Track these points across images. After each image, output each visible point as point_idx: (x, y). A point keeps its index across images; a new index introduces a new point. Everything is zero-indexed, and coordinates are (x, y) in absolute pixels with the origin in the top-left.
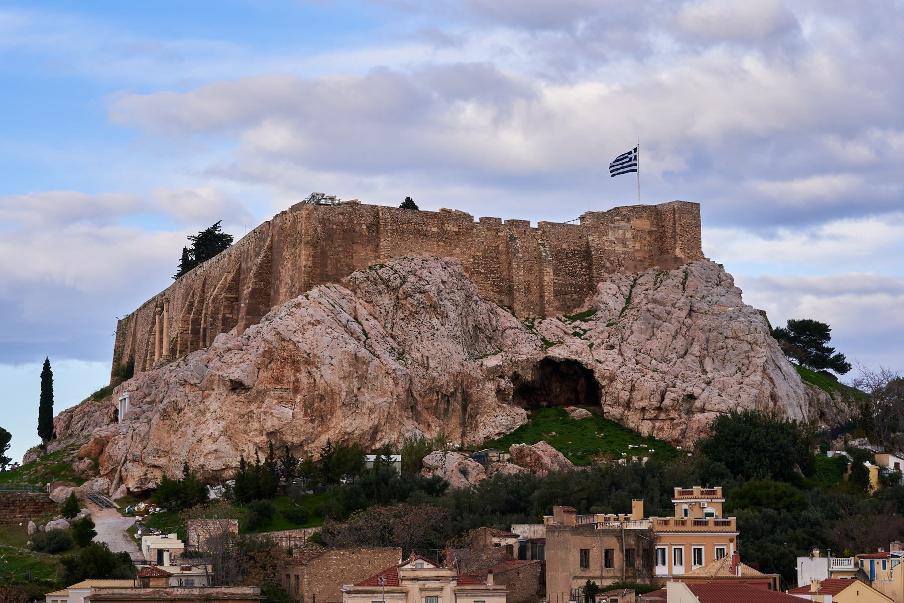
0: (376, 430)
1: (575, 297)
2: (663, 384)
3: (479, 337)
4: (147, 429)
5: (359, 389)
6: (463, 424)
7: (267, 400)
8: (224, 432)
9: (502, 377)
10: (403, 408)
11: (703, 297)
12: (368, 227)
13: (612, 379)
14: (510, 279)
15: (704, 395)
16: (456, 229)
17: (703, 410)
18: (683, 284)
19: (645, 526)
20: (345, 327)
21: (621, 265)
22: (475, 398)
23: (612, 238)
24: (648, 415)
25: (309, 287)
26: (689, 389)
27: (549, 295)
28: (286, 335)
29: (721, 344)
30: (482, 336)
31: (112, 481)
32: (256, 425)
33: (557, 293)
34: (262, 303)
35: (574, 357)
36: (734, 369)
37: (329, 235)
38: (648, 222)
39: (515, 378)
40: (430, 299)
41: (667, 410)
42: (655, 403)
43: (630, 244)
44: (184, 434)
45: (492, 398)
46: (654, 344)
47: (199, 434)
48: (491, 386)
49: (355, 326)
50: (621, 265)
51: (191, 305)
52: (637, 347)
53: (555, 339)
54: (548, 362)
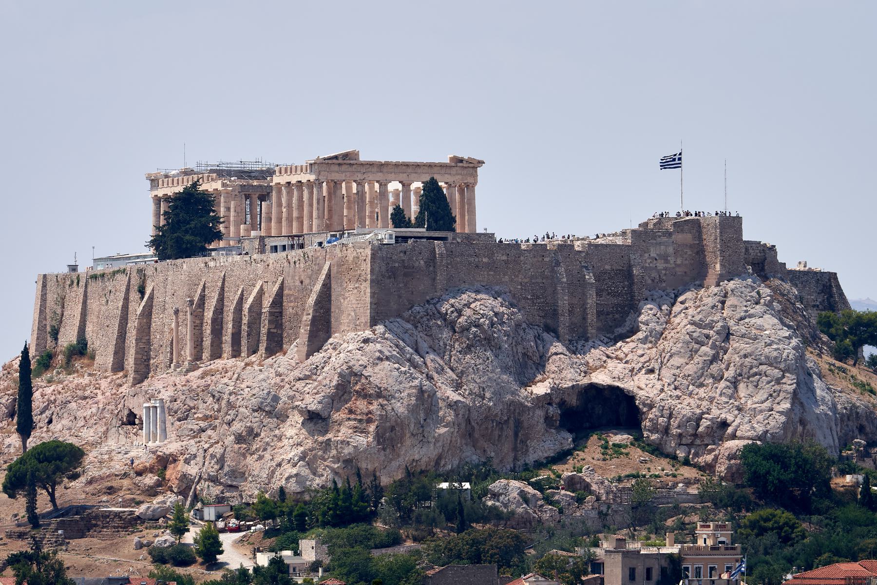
0: (440, 458)
1: (617, 316)
2: (698, 411)
4: (222, 451)
5: (425, 420)
6: (515, 449)
7: (343, 430)
8: (302, 458)
9: (550, 404)
10: (463, 436)
11: (741, 319)
12: (425, 262)
13: (651, 406)
14: (555, 304)
16: (504, 258)
17: (734, 437)
18: (723, 303)
19: (675, 550)
20: (409, 360)
21: (661, 281)
22: (525, 424)
23: (653, 255)
24: (684, 441)
25: (374, 322)
26: (723, 416)
27: (591, 317)
28: (356, 368)
29: (755, 370)
30: (530, 363)
31: (186, 498)
32: (334, 452)
33: (599, 314)
34: (321, 329)
35: (617, 384)
36: (765, 396)
37: (392, 273)
38: (689, 236)
39: (562, 404)
40: (484, 331)
41: (702, 437)
42: (691, 431)
43: (672, 259)
44: (261, 458)
45: (541, 426)
47: (278, 459)
48: (540, 413)
49: (417, 358)
50: (661, 281)
51: (202, 298)
52: (677, 372)
53: (598, 363)
54: (593, 386)
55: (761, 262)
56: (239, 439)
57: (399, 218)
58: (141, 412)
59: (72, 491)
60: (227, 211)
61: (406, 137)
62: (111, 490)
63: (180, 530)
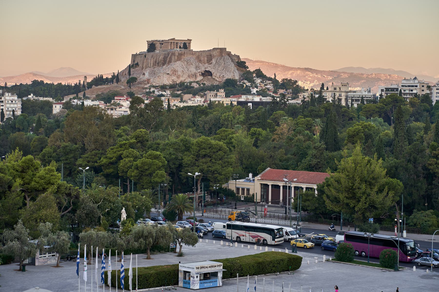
3: (197, 67)
34: (170, 62)
55: (229, 54)
60: (158, 45)
61: (181, 36)
63: (150, 89)
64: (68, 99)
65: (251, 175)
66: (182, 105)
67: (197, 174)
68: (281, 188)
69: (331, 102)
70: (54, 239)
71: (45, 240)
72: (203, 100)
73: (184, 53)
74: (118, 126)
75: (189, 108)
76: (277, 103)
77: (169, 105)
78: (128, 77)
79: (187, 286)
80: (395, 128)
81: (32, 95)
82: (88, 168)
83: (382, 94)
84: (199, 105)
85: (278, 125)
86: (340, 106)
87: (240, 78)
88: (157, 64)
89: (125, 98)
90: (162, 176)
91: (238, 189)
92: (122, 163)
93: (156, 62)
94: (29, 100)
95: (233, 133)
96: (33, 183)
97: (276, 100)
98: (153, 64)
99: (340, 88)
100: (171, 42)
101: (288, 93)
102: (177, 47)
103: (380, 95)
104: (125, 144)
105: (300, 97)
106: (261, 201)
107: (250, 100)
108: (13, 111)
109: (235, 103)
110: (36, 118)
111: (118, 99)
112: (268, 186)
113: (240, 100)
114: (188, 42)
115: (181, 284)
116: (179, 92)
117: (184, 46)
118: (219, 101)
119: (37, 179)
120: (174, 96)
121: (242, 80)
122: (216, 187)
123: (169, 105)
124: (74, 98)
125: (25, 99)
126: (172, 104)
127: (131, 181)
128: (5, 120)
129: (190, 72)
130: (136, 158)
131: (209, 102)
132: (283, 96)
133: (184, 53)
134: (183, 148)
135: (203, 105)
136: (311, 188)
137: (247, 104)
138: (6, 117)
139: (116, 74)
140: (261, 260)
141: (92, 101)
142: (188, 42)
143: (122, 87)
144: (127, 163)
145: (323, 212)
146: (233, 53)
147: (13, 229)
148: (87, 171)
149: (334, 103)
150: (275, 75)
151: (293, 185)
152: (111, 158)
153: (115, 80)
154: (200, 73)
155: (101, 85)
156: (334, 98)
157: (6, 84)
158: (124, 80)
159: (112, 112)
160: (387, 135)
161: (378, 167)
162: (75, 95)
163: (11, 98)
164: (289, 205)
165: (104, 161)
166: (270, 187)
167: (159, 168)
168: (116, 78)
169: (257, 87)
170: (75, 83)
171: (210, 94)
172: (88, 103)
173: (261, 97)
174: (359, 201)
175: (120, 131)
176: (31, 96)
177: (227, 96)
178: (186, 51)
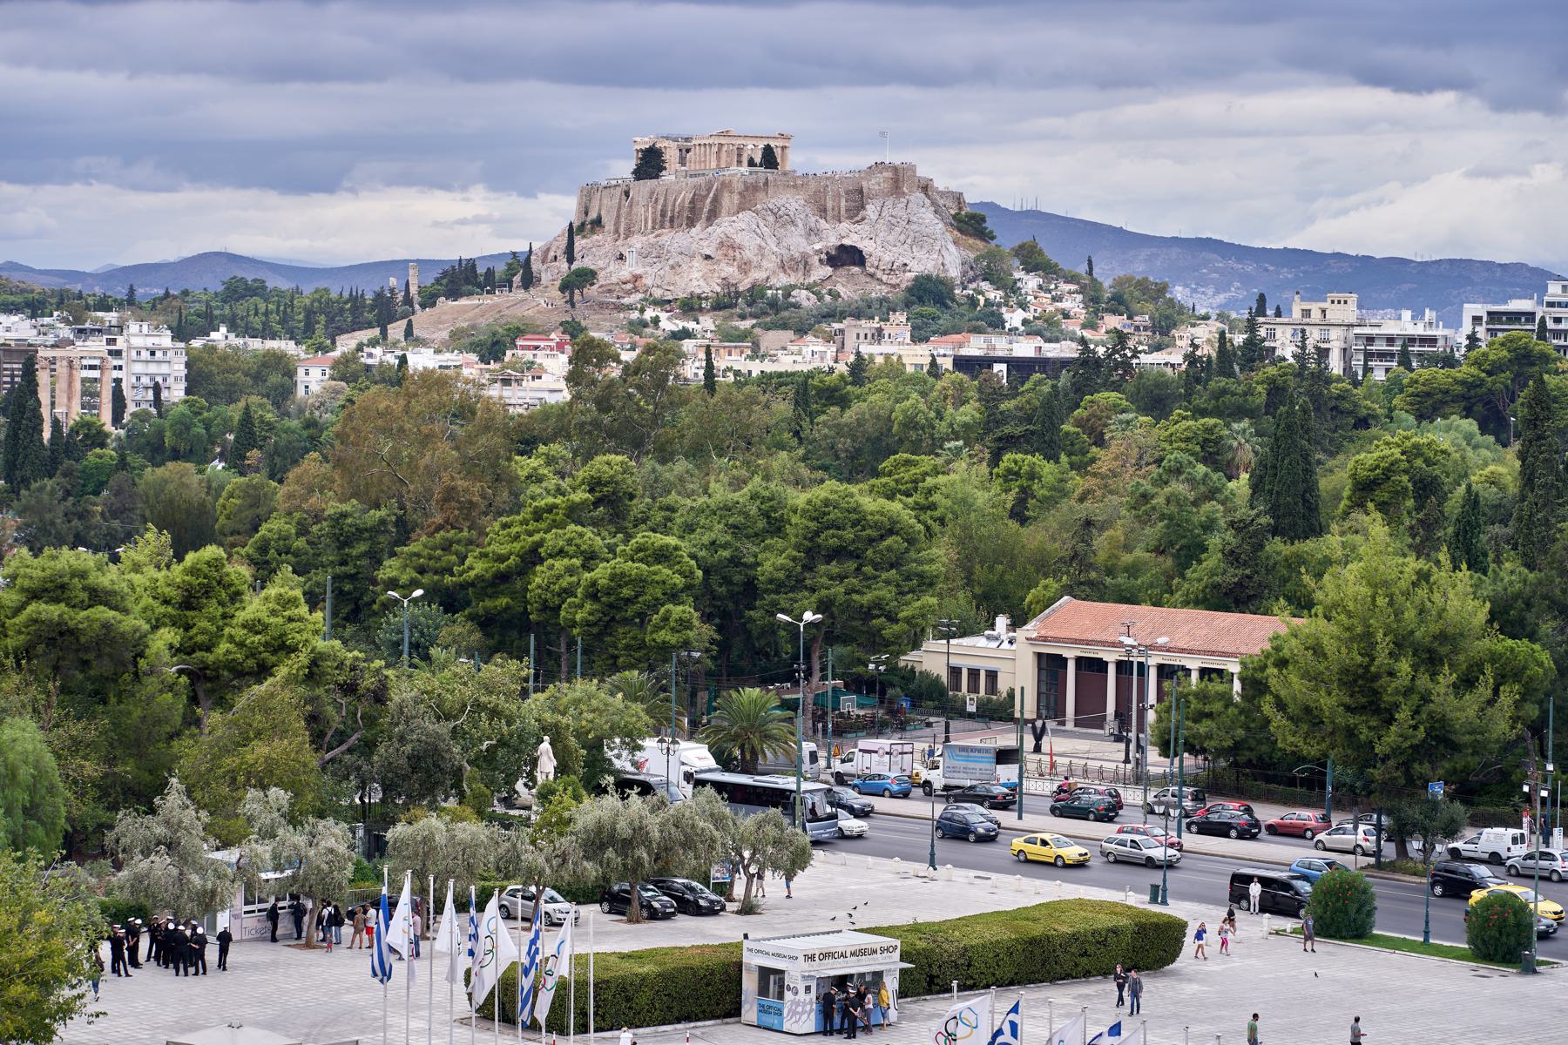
15: (913, 265)
34: (713, 215)
46: (890, 238)
55: (926, 188)
56: (672, 267)
57: (751, 163)
58: (626, 254)
59: (592, 291)
60: (671, 155)
62: (610, 291)
63: (642, 311)
64: (353, 344)
65: (1002, 622)
66: (756, 368)
67: (808, 616)
68: (1112, 670)
69: (1291, 360)
70: (295, 847)
71: (265, 850)
72: (831, 350)
73: (766, 183)
74: (527, 443)
75: (782, 379)
76: (1098, 363)
77: (709, 367)
78: (563, 265)
79: (770, 1020)
80: (1522, 456)
81: (223, 329)
82: (418, 593)
83: (1474, 333)
84: (820, 371)
85: (1100, 442)
86: (1322, 377)
87: (964, 274)
88: (667, 219)
89: (552, 344)
90: (684, 624)
91: (955, 672)
92: (540, 577)
93: (663, 215)
94: (211, 349)
95: (936, 472)
96: (224, 646)
97: (1094, 352)
98: (654, 221)
99: (1324, 311)
100: (721, 145)
101: (1137, 328)
102: (739, 162)
103: (1468, 337)
104: (550, 509)
105: (1178, 343)
106: (1039, 716)
107: (1000, 354)
108: (157, 389)
109: (947, 364)
110: (235, 412)
111: (528, 348)
112: (1062, 661)
113: (964, 352)
114: (780, 143)
115: (750, 1012)
116: (746, 324)
117: (763, 157)
118: (888, 357)
119: (240, 633)
120: (732, 337)
121: (970, 281)
122: (878, 664)
123: (709, 367)
124: (373, 343)
125: (197, 343)
126: (720, 363)
127: (571, 643)
128: (127, 418)
129: (784, 252)
130: (590, 559)
131: (852, 358)
132: (1120, 338)
133: (766, 183)
134: (761, 524)
135: (832, 371)
136: (1220, 672)
137: (990, 367)
138: (131, 408)
139: (522, 259)
140: (1037, 930)
141: (437, 351)
142: (780, 143)
143: (542, 303)
144: (559, 577)
145: (1260, 758)
146: (940, 184)
147: (152, 811)
148: (415, 601)
149: (1303, 367)
150: (1090, 262)
151: (1153, 661)
152: (502, 559)
153: (517, 279)
154: (824, 257)
155: (470, 294)
156: (1303, 348)
157: (132, 291)
158: (552, 274)
159: (508, 393)
160: (1493, 481)
161: (1461, 599)
162: (377, 331)
163: (150, 342)
164: (1141, 729)
165: (477, 567)
166: (1071, 666)
167: (674, 596)
168: (521, 270)
169: (1023, 306)
170: (377, 289)
171: (856, 331)
172: (421, 360)
173: (1039, 341)
174: (1390, 720)
175: (534, 462)
176: (220, 336)
177: (919, 337)
178: (770, 175)
